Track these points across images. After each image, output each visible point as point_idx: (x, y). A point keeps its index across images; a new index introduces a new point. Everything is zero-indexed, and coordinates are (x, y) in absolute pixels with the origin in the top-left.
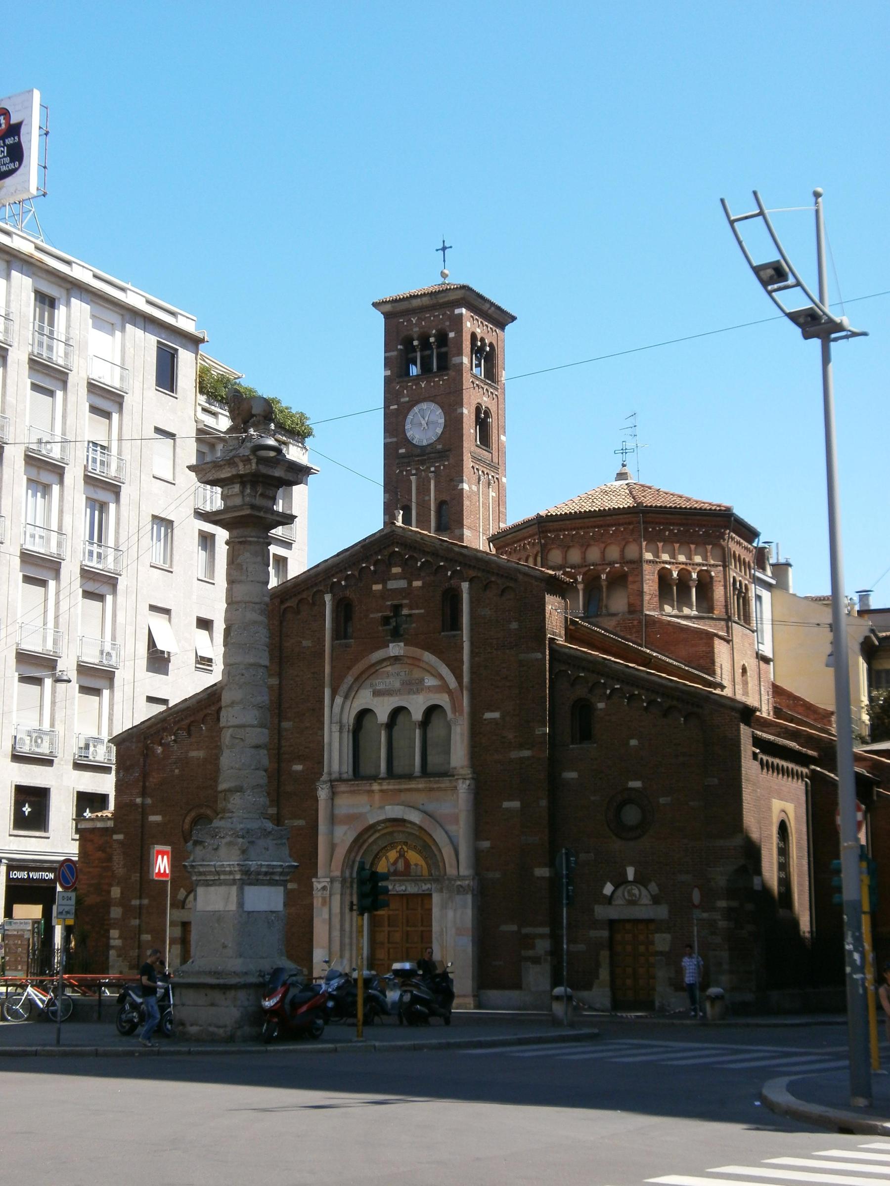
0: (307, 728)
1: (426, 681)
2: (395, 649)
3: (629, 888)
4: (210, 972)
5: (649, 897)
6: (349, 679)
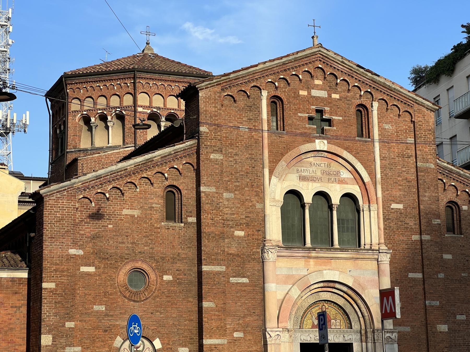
0: (247, 200)
1: (342, 173)
6: (282, 164)
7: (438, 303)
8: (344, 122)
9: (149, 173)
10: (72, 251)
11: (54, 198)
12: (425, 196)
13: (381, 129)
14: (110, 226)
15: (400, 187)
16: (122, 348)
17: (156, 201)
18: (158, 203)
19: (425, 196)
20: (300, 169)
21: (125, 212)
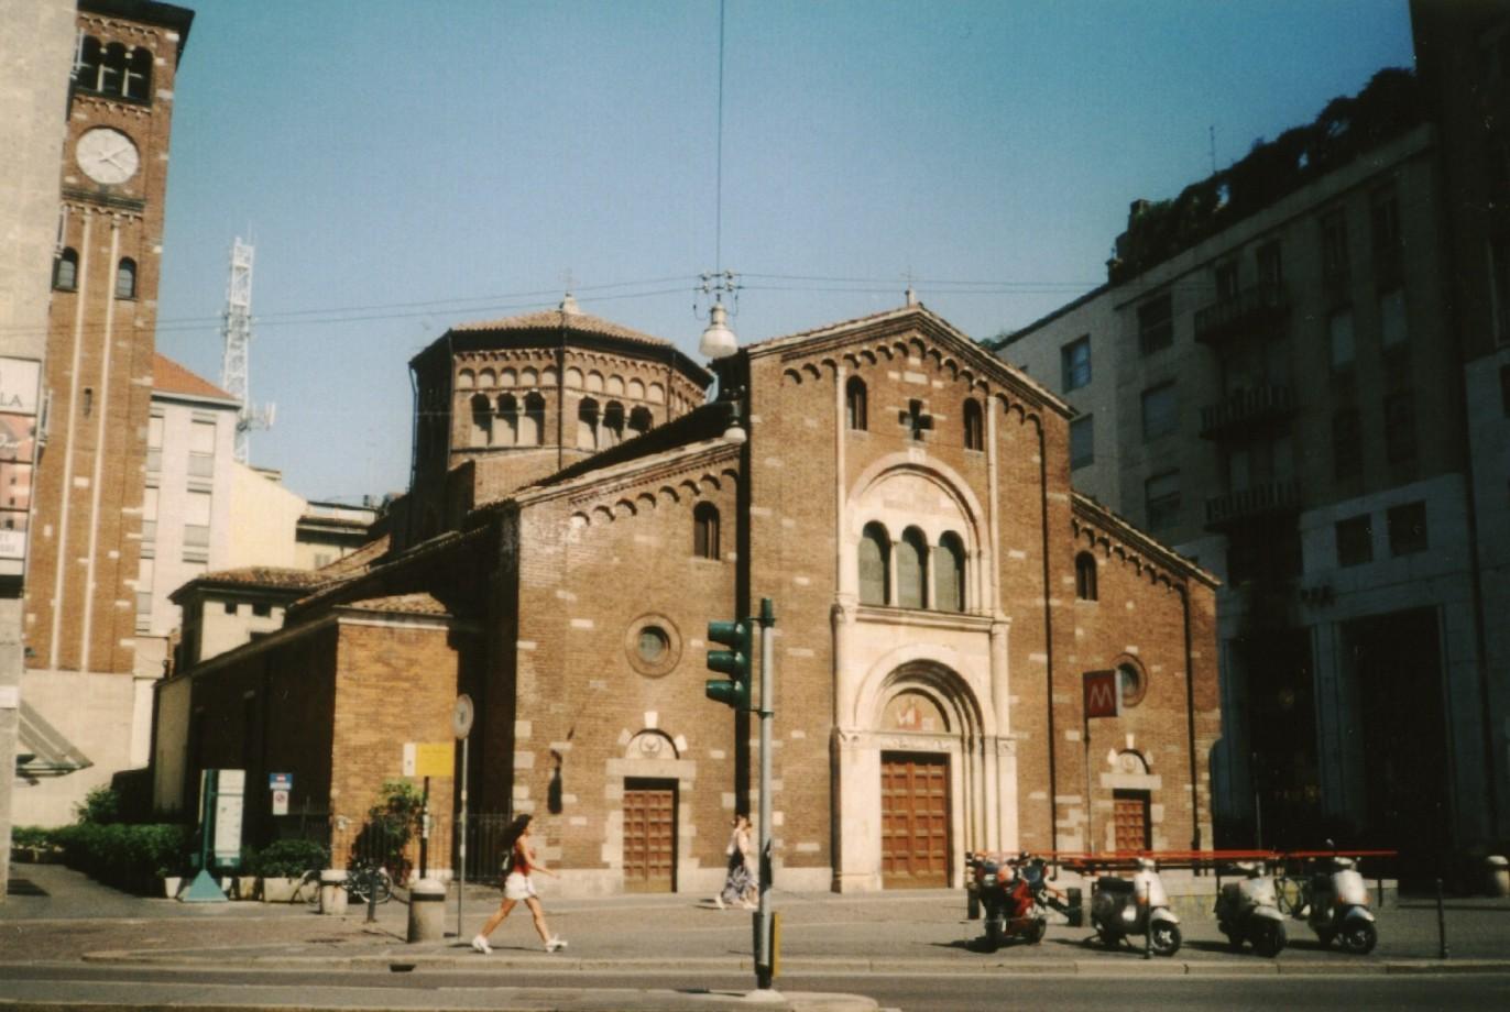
2: (916, 455)
6: (864, 479)
18: (686, 528)
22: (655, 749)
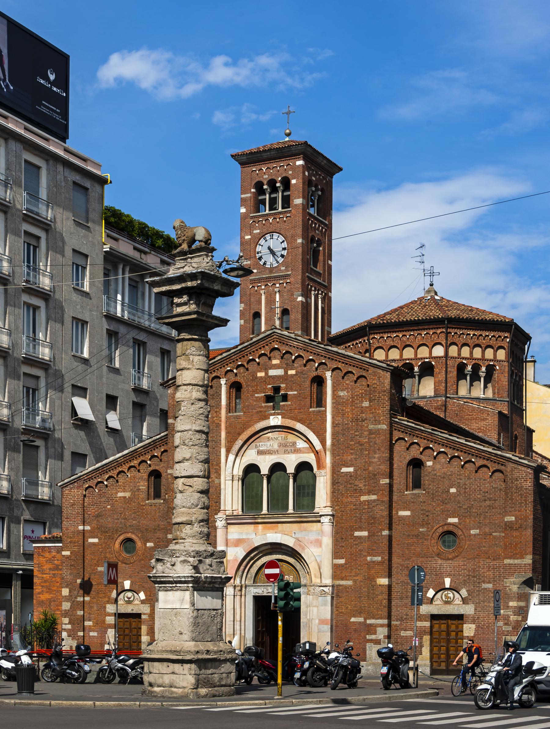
1: (298, 444)
3: (446, 592)
4: (171, 651)
5: (460, 598)
7: (379, 559)
8: (299, 395)
9: (136, 462)
10: (81, 528)
11: (69, 488)
12: (375, 458)
13: (335, 396)
14: (109, 507)
15: (352, 451)
16: (119, 599)
17: (142, 484)
18: (143, 486)
19: (375, 458)
20: (258, 444)
21: (120, 494)
22: (132, 599)
